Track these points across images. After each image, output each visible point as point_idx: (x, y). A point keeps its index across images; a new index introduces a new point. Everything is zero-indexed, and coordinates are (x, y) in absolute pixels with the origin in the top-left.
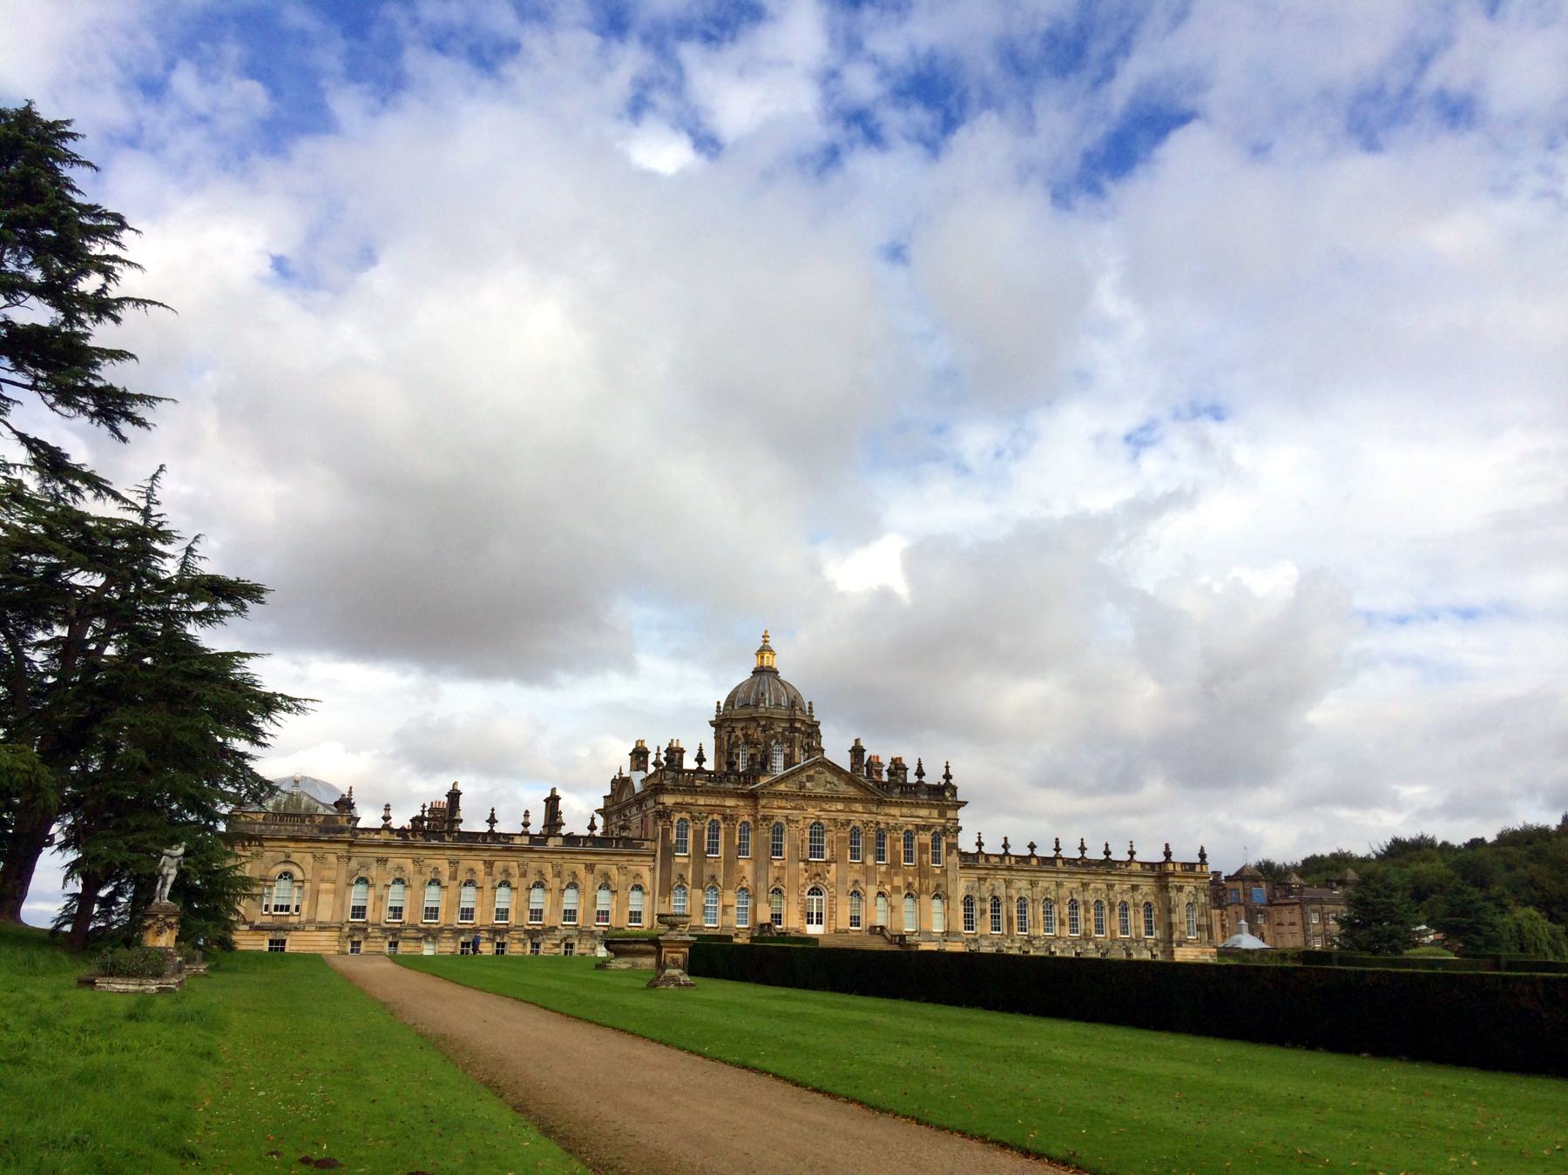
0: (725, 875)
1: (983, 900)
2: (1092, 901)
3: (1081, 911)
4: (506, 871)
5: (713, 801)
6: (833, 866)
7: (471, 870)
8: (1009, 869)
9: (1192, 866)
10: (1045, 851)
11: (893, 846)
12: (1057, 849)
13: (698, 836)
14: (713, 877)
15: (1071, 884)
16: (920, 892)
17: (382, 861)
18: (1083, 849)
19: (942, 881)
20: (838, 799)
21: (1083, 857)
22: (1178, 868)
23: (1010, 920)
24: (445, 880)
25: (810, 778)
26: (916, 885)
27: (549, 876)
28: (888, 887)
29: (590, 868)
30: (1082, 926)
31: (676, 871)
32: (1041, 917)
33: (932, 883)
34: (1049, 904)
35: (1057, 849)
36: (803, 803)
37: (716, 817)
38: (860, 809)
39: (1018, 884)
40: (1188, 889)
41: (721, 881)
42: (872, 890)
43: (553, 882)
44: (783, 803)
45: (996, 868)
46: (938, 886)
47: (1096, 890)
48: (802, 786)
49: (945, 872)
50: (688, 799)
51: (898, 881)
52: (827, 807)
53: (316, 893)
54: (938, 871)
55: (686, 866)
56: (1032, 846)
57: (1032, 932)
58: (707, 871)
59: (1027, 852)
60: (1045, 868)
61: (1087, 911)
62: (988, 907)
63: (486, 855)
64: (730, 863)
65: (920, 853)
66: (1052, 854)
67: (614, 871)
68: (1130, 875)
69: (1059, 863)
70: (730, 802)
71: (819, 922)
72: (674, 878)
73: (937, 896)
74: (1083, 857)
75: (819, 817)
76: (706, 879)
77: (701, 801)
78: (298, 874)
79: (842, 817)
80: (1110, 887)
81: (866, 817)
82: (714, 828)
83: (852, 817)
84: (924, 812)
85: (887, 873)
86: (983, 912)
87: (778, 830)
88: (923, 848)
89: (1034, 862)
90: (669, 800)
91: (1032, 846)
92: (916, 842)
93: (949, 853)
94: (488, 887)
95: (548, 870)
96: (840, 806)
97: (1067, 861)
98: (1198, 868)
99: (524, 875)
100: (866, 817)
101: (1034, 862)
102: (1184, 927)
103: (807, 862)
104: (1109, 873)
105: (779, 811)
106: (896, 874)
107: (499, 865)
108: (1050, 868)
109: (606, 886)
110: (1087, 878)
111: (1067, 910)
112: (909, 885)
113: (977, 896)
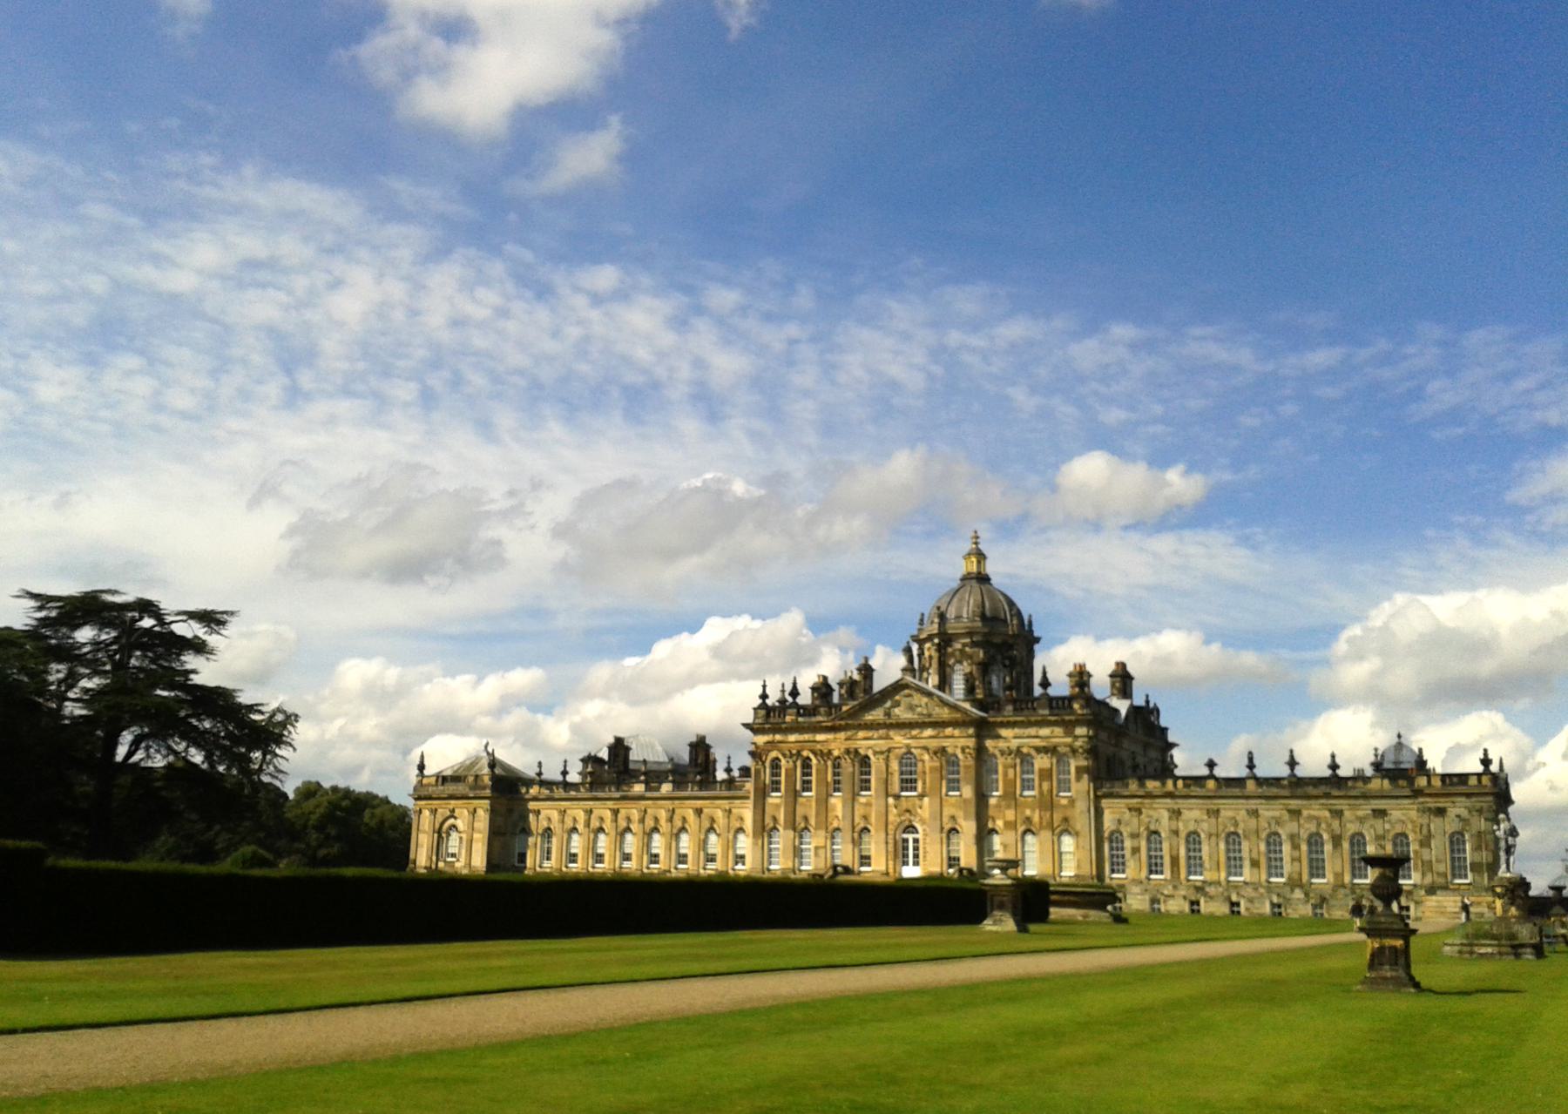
0: (817, 814)
1: (1135, 836)
2: (1304, 835)
3: (1286, 848)
4: (629, 820)
5: (806, 737)
6: (926, 799)
7: (602, 819)
8: (1170, 795)
9: (1463, 778)
10: (1231, 767)
11: (1005, 774)
12: (1251, 766)
13: (791, 774)
14: (806, 819)
15: (1270, 811)
16: (1041, 828)
17: (538, 813)
18: (1292, 763)
19: (1069, 813)
20: (922, 725)
21: (1293, 775)
22: (1437, 782)
23: (1175, 861)
24: (580, 827)
25: (897, 704)
26: (1036, 819)
27: (663, 822)
28: (1000, 823)
29: (699, 812)
30: (1287, 868)
31: (769, 811)
32: (1223, 858)
33: (1057, 817)
34: (1233, 838)
35: (1251, 766)
36: (892, 733)
37: (805, 753)
38: (957, 732)
39: (1186, 814)
40: (1452, 812)
41: (812, 821)
42: (968, 827)
43: (664, 826)
44: (870, 734)
45: (1150, 796)
46: (1066, 820)
47: (1311, 818)
48: (888, 714)
49: (1072, 801)
50: (778, 737)
51: (1010, 815)
52: (914, 732)
53: (471, 841)
54: (1064, 802)
55: (777, 806)
56: (1211, 764)
57: (1208, 875)
58: (800, 811)
59: (1205, 771)
60: (1224, 791)
61: (1296, 847)
62: (1143, 844)
63: (610, 804)
64: (823, 803)
65: (1041, 779)
66: (1244, 772)
67: (719, 814)
68: (1366, 797)
69: (1251, 785)
70: (820, 737)
71: (916, 863)
72: (768, 820)
73: (1066, 831)
74: (1293, 775)
75: (908, 746)
76: (798, 819)
77: (792, 738)
78: (460, 824)
79: (934, 744)
80: (1338, 814)
81: (962, 742)
82: (806, 764)
83: (946, 743)
84: (1045, 731)
85: (998, 806)
86: (1136, 850)
87: (865, 762)
88: (1046, 775)
89: (1211, 784)
90: (762, 739)
91: (1211, 764)
92: (1036, 767)
93: (1078, 779)
94: (613, 833)
95: (663, 815)
96: (929, 732)
97: (1262, 782)
98: (1473, 781)
99: (642, 821)
100: (962, 742)
101: (1211, 784)
102: (1444, 867)
103: (897, 797)
104: (1327, 796)
105: (866, 743)
106: (1008, 807)
107: (623, 813)
108: (1237, 791)
109: (711, 829)
110: (1294, 804)
111: (1263, 847)
112: (1028, 820)
113: (1126, 831)
